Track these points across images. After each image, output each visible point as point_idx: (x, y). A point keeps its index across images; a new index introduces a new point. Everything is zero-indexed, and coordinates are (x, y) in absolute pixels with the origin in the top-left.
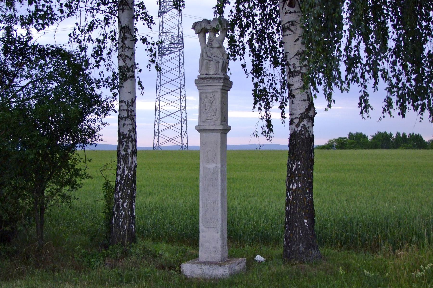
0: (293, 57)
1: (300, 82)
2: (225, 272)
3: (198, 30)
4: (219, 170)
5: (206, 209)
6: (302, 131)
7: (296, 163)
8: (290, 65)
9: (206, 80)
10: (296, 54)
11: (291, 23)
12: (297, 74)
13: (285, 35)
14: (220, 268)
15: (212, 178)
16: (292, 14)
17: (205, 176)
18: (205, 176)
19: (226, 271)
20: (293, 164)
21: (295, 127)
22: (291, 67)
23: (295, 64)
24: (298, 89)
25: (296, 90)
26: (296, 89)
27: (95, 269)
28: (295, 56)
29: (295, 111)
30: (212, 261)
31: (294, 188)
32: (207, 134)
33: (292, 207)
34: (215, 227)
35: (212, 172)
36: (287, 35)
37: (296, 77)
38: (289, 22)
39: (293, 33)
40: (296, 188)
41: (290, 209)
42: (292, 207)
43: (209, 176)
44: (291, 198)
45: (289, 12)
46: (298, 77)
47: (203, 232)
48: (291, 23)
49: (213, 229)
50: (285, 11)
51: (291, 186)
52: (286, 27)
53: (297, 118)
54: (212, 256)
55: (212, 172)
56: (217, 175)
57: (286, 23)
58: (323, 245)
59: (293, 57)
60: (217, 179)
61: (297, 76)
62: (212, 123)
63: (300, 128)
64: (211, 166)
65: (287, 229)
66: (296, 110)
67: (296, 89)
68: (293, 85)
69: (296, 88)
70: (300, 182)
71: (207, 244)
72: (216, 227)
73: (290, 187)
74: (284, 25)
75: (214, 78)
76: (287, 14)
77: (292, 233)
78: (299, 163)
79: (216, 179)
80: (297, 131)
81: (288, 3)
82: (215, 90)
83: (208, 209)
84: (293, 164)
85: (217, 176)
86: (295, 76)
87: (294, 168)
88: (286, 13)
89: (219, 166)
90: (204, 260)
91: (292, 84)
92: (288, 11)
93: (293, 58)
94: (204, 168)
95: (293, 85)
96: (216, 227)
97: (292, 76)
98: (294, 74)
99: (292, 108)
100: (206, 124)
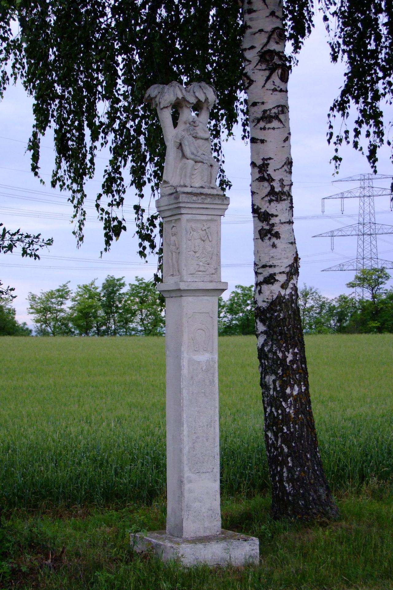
0: (281, 168)
1: (287, 211)
2: (253, 550)
3: (168, 100)
4: (216, 365)
5: (194, 438)
6: (293, 295)
7: (291, 350)
8: (273, 180)
9: (200, 198)
10: (285, 163)
11: (280, 109)
12: (285, 197)
13: (269, 128)
14: (245, 543)
15: (204, 381)
16: (282, 93)
17: (192, 378)
18: (192, 378)
19: (255, 548)
20: (286, 353)
21: (281, 289)
22: (275, 184)
23: (283, 180)
24: (285, 223)
25: (281, 225)
26: (282, 223)
27: (171, 566)
28: (283, 166)
29: (279, 261)
30: (205, 534)
31: (295, 393)
32: (195, 298)
33: (297, 426)
34: (209, 471)
35: (204, 368)
36: (274, 129)
37: (283, 202)
38: (278, 106)
39: (282, 126)
40: (298, 394)
41: (292, 430)
42: (297, 426)
43: (200, 376)
44: (291, 412)
45: (279, 89)
46: (286, 202)
47: (190, 482)
48: (280, 109)
49: (207, 474)
50: (273, 87)
51: (288, 391)
52: (273, 115)
53: (283, 272)
54: (206, 526)
55: (204, 368)
56: (213, 374)
57: (274, 108)
58: (195, 499)
59: (281, 168)
60: (214, 382)
61: (285, 200)
62: (208, 278)
63: (288, 291)
64: (203, 357)
65: (290, 464)
66: (280, 259)
67: (282, 223)
68: (277, 216)
69: (282, 221)
70: (302, 383)
71: (197, 505)
72: (212, 471)
73: (286, 393)
74: (270, 110)
75: (206, 195)
76: (276, 93)
77: (304, 472)
78: (296, 350)
79: (212, 382)
80: (285, 295)
81: (279, 74)
82: (213, 217)
83: (197, 438)
84: (286, 353)
85: (213, 377)
86: (281, 200)
87: (288, 360)
88: (274, 90)
89: (216, 357)
90: (192, 535)
91: (275, 214)
92: (279, 87)
93: (280, 170)
94: (190, 361)
95: (277, 216)
96: (212, 471)
97: (277, 201)
98: (281, 198)
99: (272, 255)
100: (197, 280)
